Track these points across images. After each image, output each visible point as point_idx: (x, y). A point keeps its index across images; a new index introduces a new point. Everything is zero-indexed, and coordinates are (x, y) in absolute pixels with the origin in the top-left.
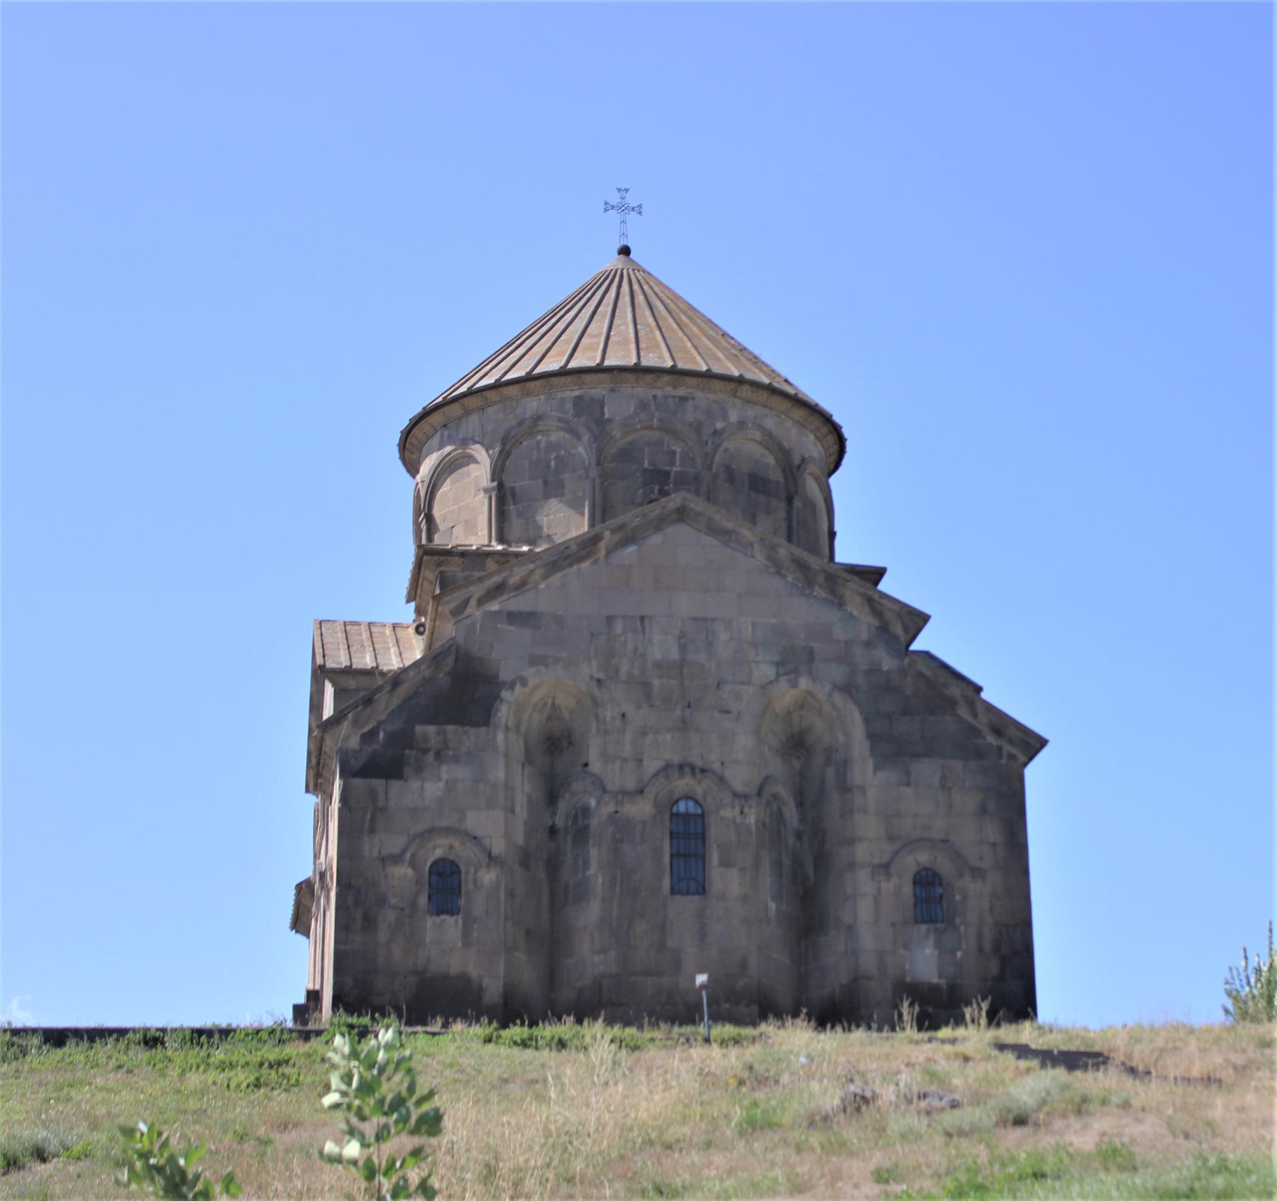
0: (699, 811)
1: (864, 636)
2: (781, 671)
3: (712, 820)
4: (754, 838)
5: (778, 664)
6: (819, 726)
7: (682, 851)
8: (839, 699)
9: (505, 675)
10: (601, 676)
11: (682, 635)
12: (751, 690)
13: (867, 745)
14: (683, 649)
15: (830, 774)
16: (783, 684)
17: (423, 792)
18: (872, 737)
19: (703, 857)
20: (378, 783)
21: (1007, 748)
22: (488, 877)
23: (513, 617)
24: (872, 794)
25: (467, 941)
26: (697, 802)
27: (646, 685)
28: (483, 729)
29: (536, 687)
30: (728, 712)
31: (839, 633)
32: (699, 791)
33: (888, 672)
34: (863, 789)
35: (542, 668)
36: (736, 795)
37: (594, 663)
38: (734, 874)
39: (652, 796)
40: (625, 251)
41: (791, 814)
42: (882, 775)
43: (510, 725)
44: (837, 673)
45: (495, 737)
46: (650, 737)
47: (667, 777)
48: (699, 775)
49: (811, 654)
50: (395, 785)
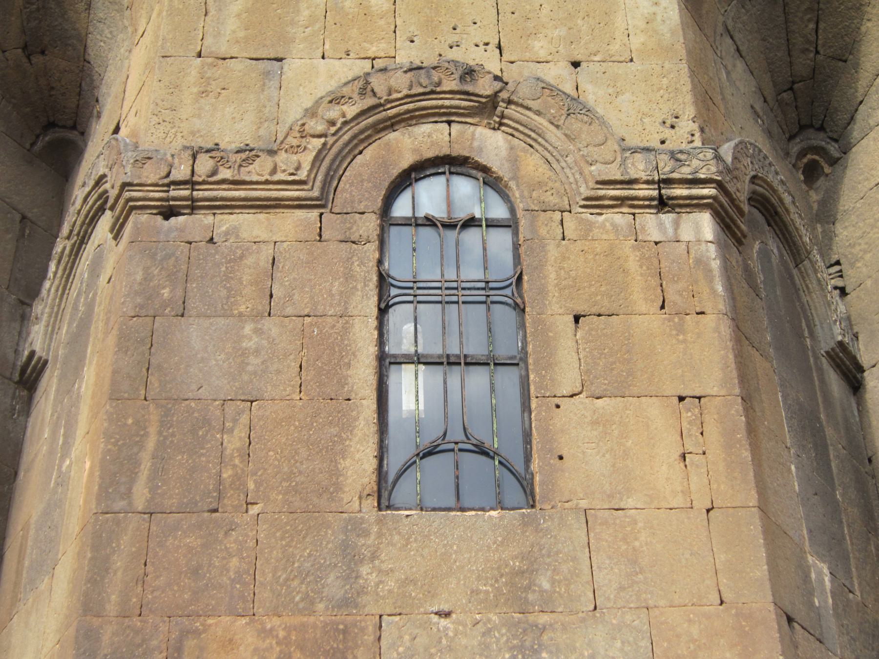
4: (720, 288)
38: (656, 414)
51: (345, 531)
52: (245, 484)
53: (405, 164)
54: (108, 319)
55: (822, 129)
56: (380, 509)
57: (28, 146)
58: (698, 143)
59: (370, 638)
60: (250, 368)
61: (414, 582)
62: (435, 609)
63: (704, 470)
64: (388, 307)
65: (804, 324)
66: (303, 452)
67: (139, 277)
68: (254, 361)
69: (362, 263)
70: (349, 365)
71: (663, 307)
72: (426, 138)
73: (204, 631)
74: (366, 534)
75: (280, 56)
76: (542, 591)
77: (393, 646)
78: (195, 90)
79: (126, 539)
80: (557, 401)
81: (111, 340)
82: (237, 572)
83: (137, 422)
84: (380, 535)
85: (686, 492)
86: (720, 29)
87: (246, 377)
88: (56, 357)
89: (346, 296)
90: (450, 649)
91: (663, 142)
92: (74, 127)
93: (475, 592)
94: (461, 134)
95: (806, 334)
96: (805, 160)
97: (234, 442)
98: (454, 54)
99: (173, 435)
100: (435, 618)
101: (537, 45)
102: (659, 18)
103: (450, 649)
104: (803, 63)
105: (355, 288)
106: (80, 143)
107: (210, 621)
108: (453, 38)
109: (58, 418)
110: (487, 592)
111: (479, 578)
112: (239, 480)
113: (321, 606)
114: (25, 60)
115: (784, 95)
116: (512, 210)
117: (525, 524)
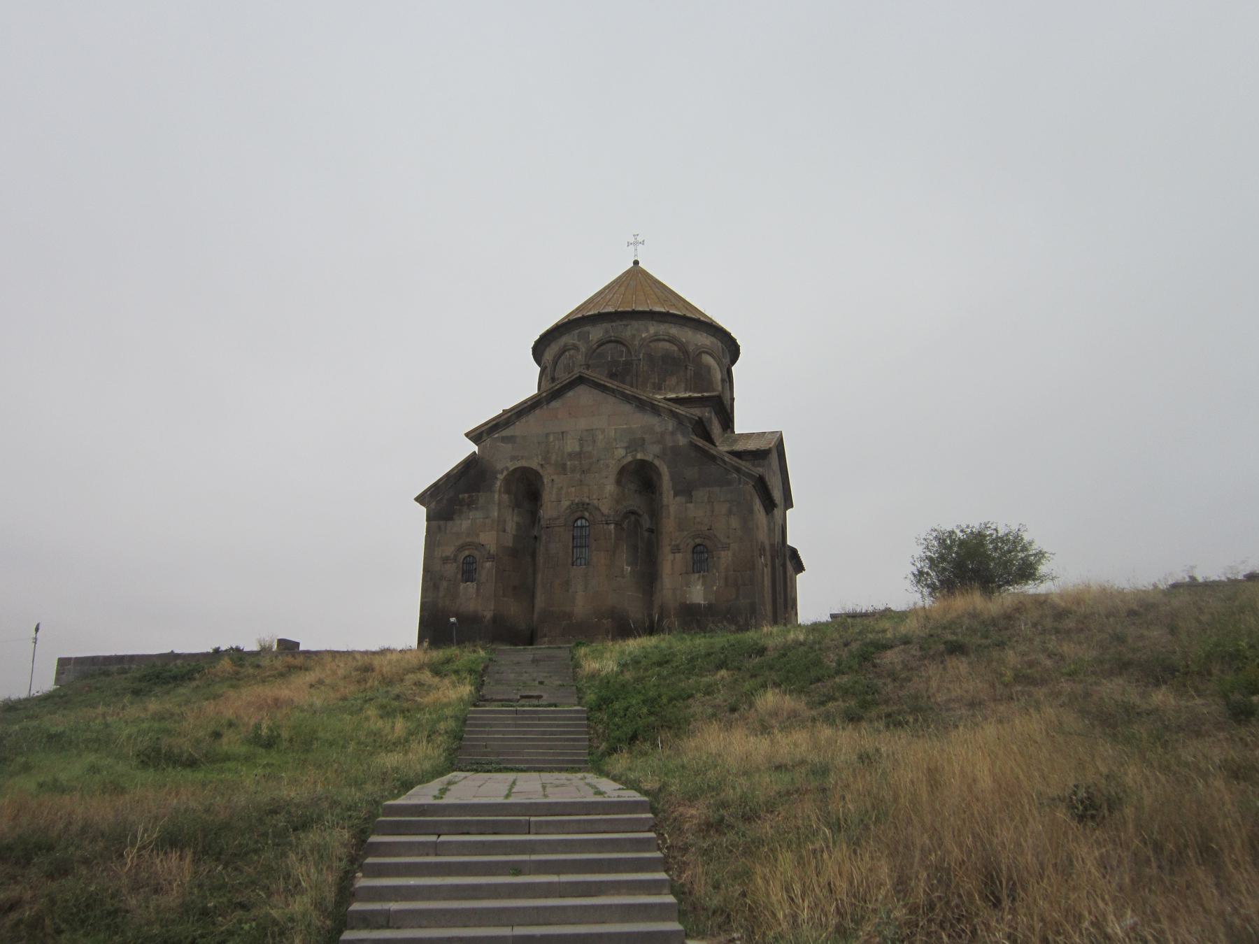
1: (670, 428)
5: (626, 448)
11: (581, 440)
14: (581, 446)
17: (463, 524)
20: (442, 523)
21: (743, 478)
22: (488, 565)
23: (504, 439)
24: (672, 509)
25: (477, 595)
27: (565, 464)
31: (658, 429)
32: (587, 514)
40: (636, 263)
41: (646, 522)
42: (678, 499)
49: (643, 439)
50: (450, 523)
72: (579, 514)
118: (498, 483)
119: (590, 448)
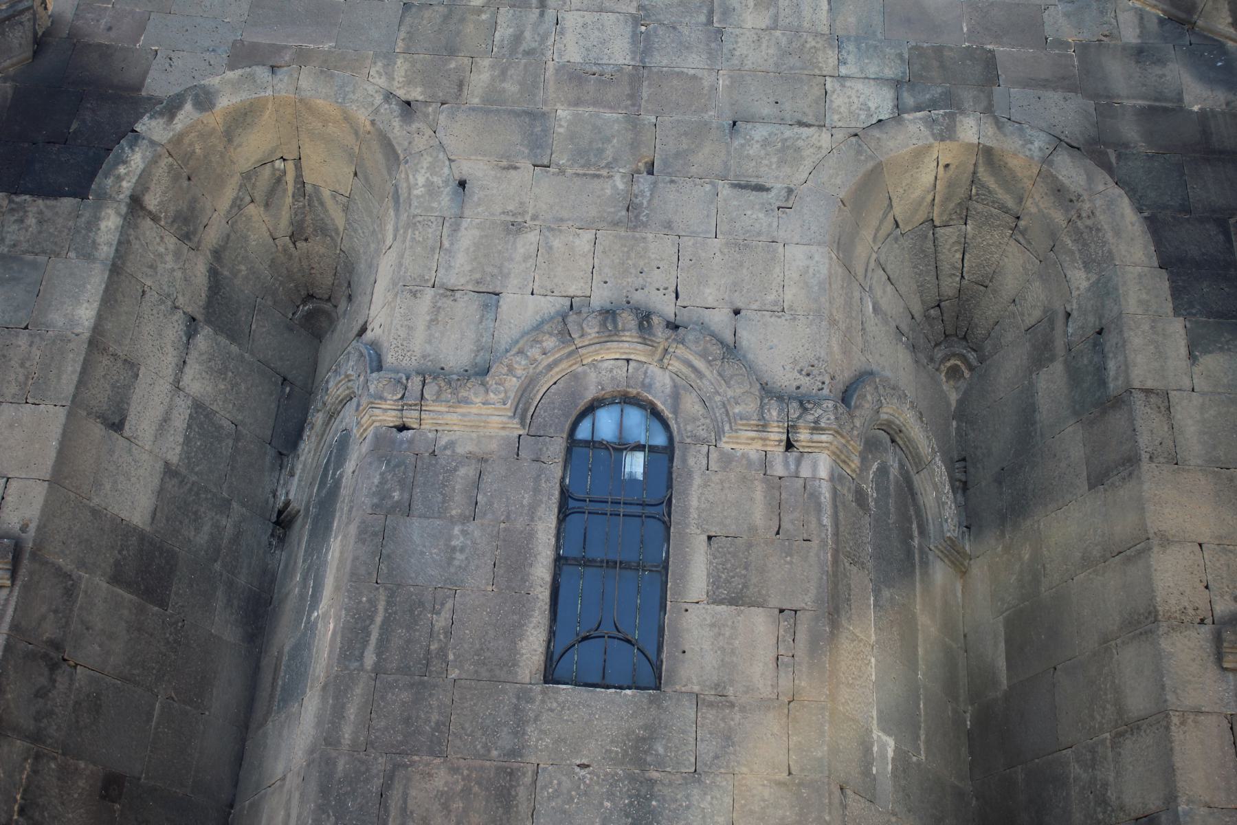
0: (660, 440)
1: (1130, 35)
2: (909, 100)
3: (693, 460)
4: (826, 520)
5: (897, 84)
6: (1013, 264)
7: (595, 553)
8: (1071, 172)
9: (158, 84)
10: (416, 94)
12: (825, 139)
13: (1163, 284)
14: (643, 45)
15: (1051, 384)
16: (915, 129)
18: (1169, 262)
19: (655, 574)
26: (655, 414)
27: (534, 121)
28: (67, 203)
29: (242, 118)
30: (760, 188)
33: (1203, 112)
34: (1162, 399)
35: (262, 73)
36: (768, 392)
37: (401, 67)
39: (513, 383)
42: (1212, 362)
43: (152, 201)
44: (1066, 112)
45: (93, 224)
46: (532, 237)
47: (565, 335)
48: (660, 333)
49: (990, 62)
51: (518, 698)
52: (446, 656)
53: (590, 394)
54: (352, 507)
55: (965, 338)
56: (546, 682)
57: (290, 315)
58: (826, 392)
59: (528, 779)
60: (456, 563)
61: (564, 741)
62: (578, 762)
63: (791, 669)
64: (566, 516)
65: (914, 526)
66: (492, 633)
67: (376, 481)
68: (458, 555)
69: (547, 480)
70: (531, 565)
71: (778, 533)
73: (411, 765)
74: (531, 700)
75: (497, 290)
76: (657, 755)
77: (545, 787)
78: (428, 318)
79: (358, 691)
80: (686, 606)
81: (353, 529)
82: (437, 723)
83: (369, 601)
84: (543, 701)
85: (775, 686)
86: (872, 264)
87: (452, 570)
88: (307, 509)
89: (533, 509)
90: (586, 794)
91: (798, 388)
92: (329, 300)
93: (610, 751)
94: (637, 370)
95: (916, 533)
96: (948, 364)
97: (441, 622)
98: (638, 297)
99: (395, 613)
100: (577, 769)
101: (708, 291)
102: (811, 271)
103: (586, 794)
104: (949, 285)
105: (541, 501)
106: (334, 315)
107: (416, 758)
108: (640, 281)
109: (309, 569)
110: (617, 753)
111: (612, 742)
112: (442, 653)
113: (495, 753)
114: (291, 245)
115: (932, 311)
116: (671, 439)
117: (651, 702)
118: (137, 159)
119: (694, 63)
